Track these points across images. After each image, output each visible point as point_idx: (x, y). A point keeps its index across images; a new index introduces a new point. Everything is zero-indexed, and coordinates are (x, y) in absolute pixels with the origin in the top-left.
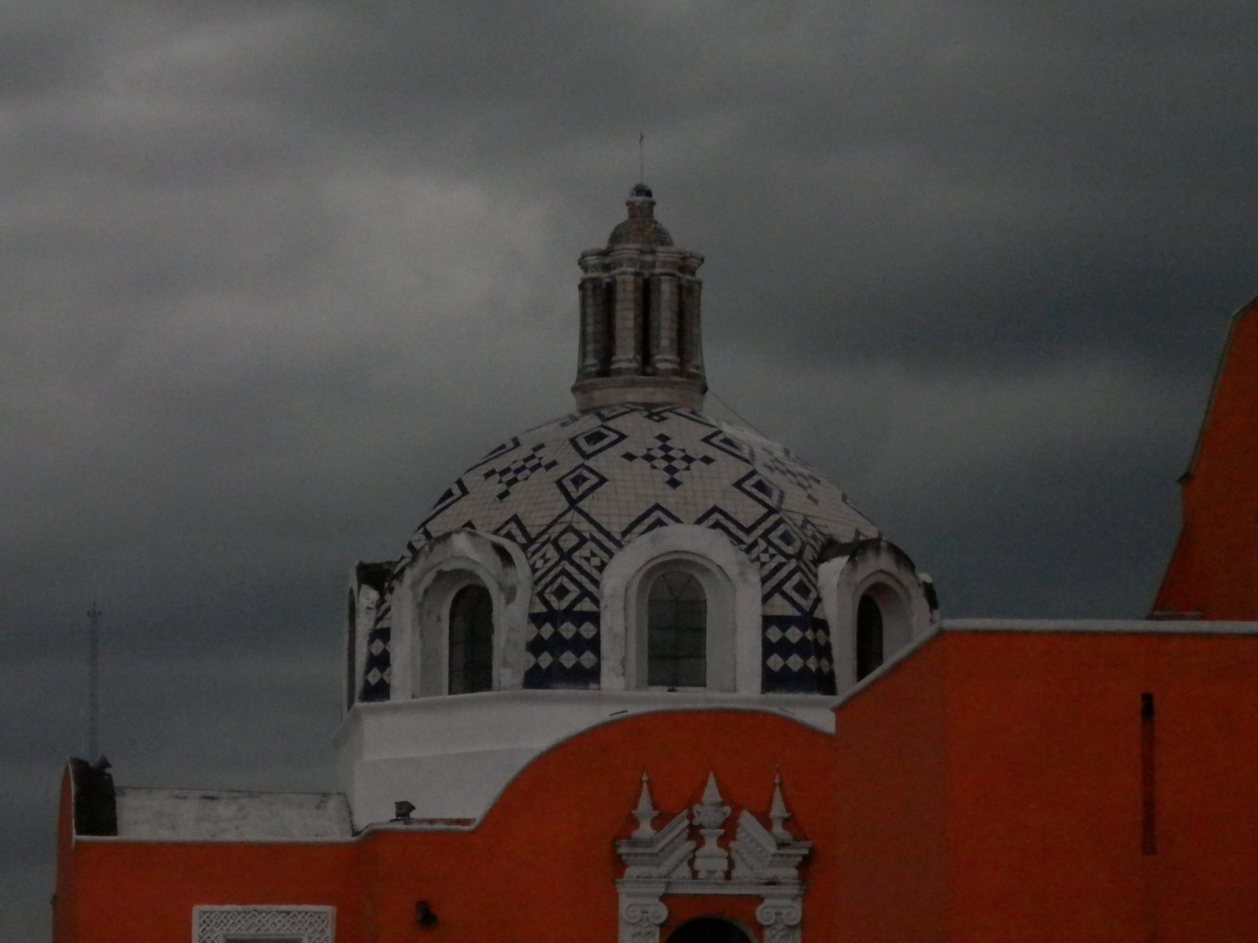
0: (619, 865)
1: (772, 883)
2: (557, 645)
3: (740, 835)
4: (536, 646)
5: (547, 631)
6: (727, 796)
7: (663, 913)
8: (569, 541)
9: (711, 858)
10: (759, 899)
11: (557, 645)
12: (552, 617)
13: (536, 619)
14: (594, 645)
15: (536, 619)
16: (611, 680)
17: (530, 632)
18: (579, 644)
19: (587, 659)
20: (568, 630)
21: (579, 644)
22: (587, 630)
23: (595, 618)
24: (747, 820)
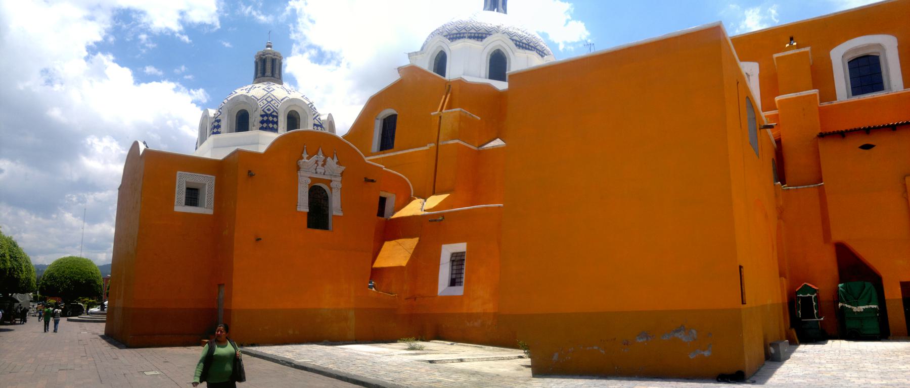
0: (298, 168)
1: (335, 176)
2: (268, 122)
3: (327, 164)
4: (262, 122)
5: (265, 118)
6: (324, 155)
7: (309, 181)
8: (269, 100)
9: (320, 170)
10: (331, 181)
11: (268, 122)
12: (267, 115)
13: (262, 116)
14: (277, 123)
15: (262, 116)
16: (279, 130)
17: (261, 119)
18: (273, 122)
19: (275, 126)
20: (271, 119)
21: (273, 122)
22: (275, 119)
23: (277, 117)
24: (329, 159)
